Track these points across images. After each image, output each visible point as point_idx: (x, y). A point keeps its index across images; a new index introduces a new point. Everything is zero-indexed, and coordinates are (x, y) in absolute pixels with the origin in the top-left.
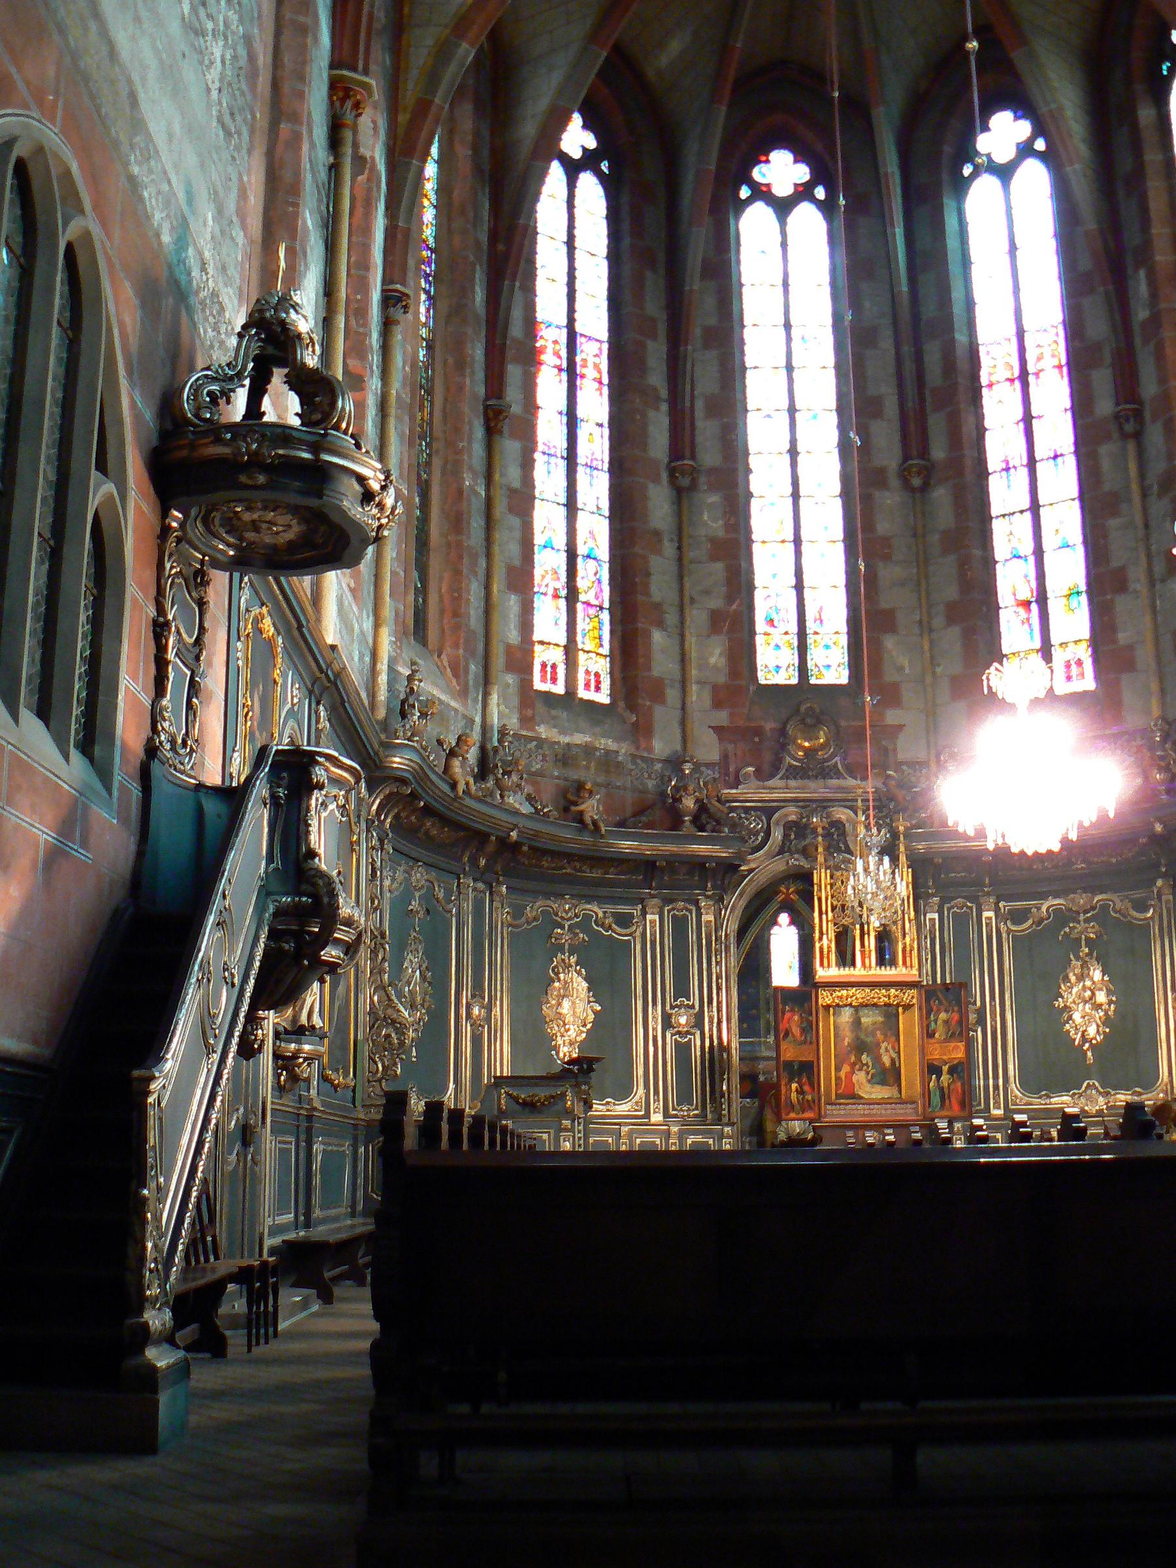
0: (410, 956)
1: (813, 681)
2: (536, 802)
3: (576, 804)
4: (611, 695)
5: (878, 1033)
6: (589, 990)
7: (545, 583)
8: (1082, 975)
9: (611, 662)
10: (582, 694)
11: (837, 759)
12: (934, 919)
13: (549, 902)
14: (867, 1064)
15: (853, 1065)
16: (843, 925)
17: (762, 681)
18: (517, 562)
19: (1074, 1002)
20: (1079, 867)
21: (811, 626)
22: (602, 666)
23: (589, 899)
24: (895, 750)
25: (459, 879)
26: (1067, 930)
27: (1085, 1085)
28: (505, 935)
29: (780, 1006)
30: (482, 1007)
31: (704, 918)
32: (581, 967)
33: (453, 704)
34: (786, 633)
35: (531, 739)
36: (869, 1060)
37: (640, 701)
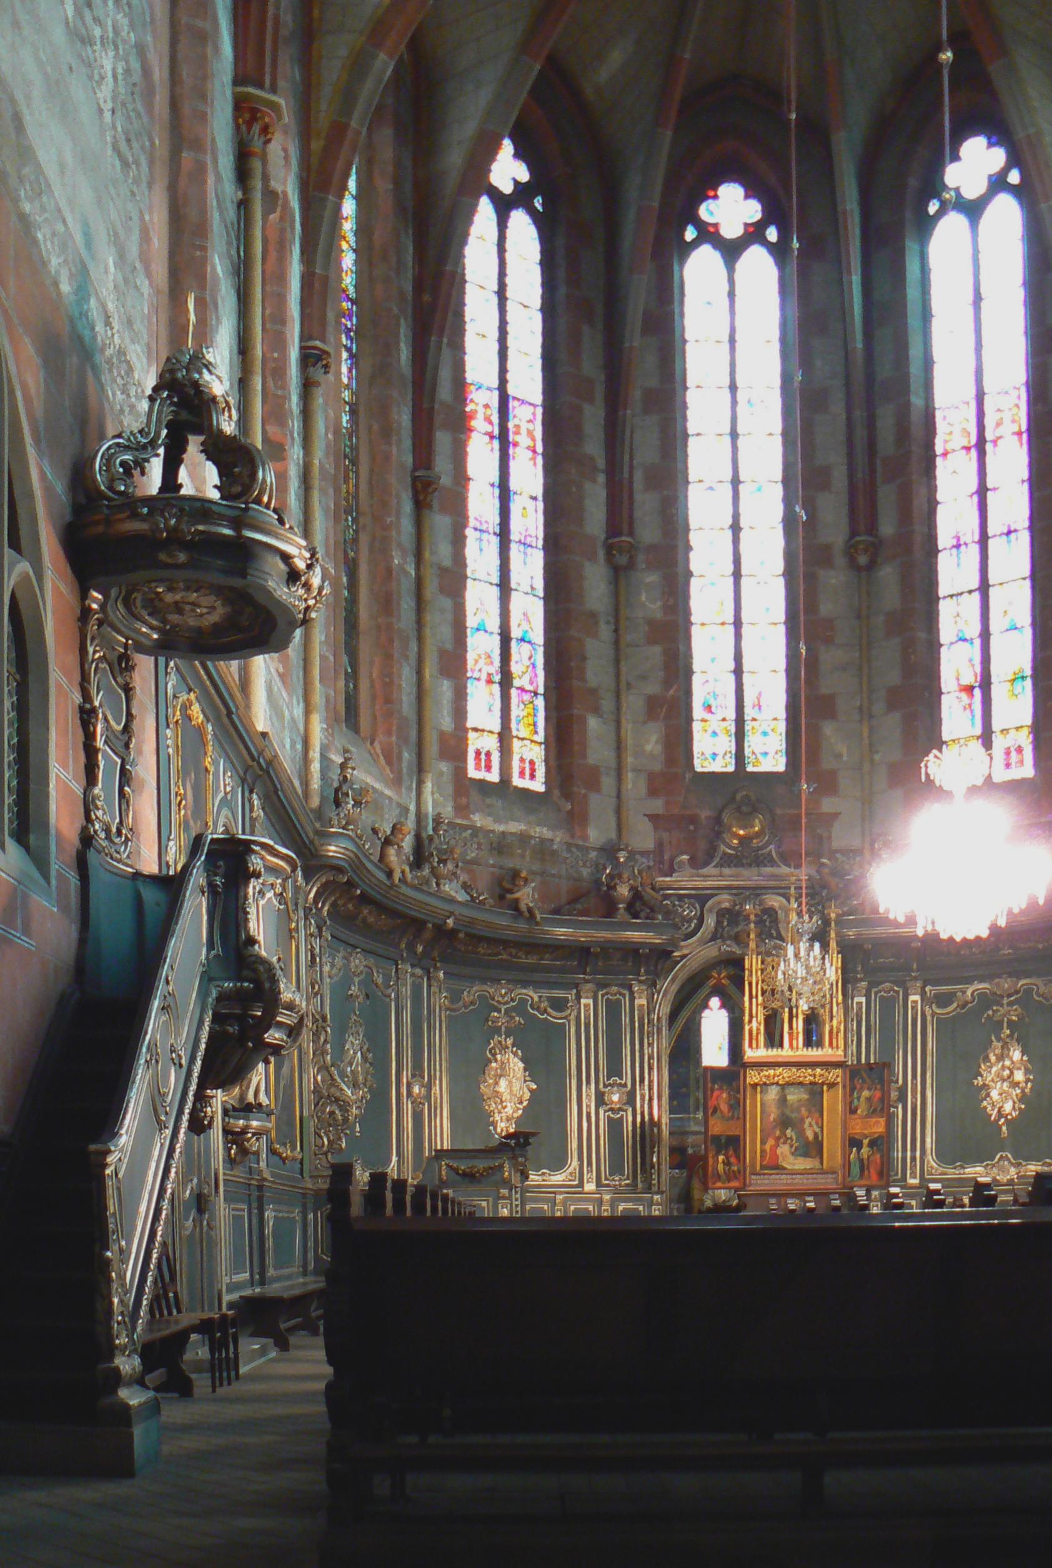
0: (351, 1038)
1: (750, 768)
2: (472, 889)
3: (511, 892)
4: (546, 783)
5: (803, 1109)
7: (477, 668)
9: (546, 750)
10: (517, 782)
11: (772, 847)
12: (861, 1003)
13: (485, 987)
14: (791, 1138)
15: (778, 1139)
16: (773, 1009)
17: (698, 769)
18: (449, 646)
19: (993, 1080)
21: (749, 713)
22: (537, 754)
24: (830, 838)
25: (397, 965)
27: (998, 1156)
29: (710, 1085)
33: (387, 792)
34: (724, 720)
35: (465, 828)
36: (793, 1134)
37: (576, 789)
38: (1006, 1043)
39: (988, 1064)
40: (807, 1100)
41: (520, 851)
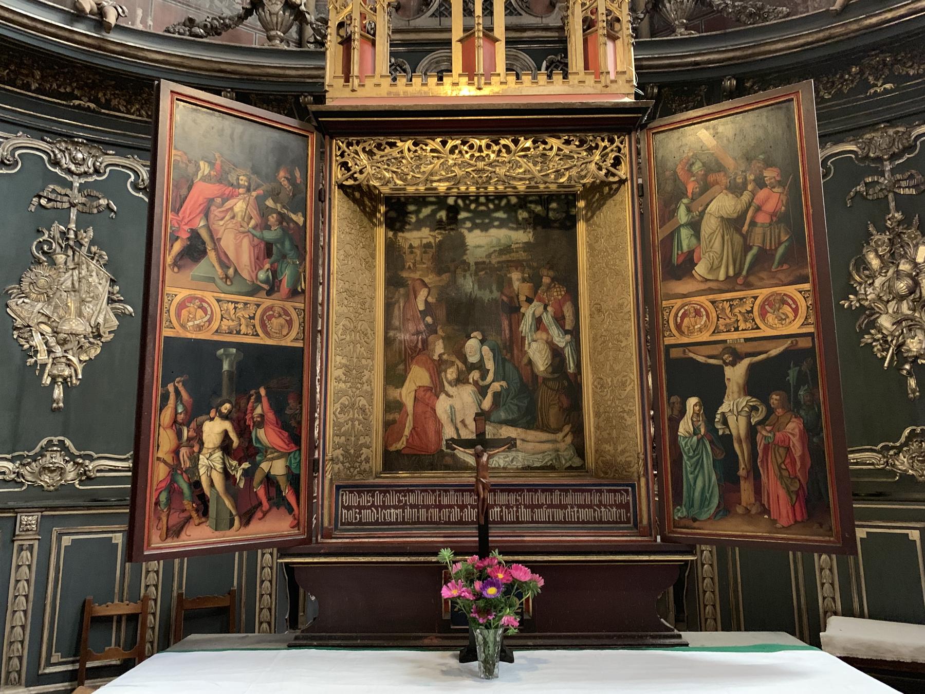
6: (113, 282)
14: (480, 366)
15: (438, 367)
27: (907, 432)
38: (899, 235)
39: (867, 272)
40: (527, 247)
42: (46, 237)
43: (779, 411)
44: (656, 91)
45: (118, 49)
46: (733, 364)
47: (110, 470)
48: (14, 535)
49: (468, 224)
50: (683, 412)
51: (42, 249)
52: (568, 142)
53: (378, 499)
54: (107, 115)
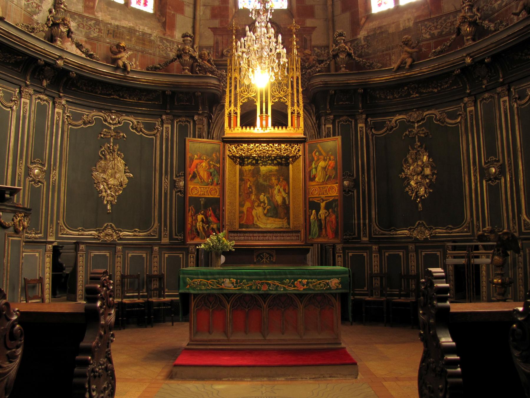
6: (126, 165)
8: (416, 158)
14: (264, 202)
15: (253, 203)
16: (248, 98)
19: (411, 174)
20: (414, 96)
23: (128, 114)
24: (311, 40)
26: (407, 133)
27: (417, 223)
28: (66, 129)
30: (41, 170)
31: (197, 126)
32: (121, 152)
35: (91, 19)
37: (168, 10)
38: (418, 151)
39: (408, 164)
40: (277, 170)
41: (128, 37)
42: (103, 149)
43: (331, 213)
44: (333, 92)
45: (131, 79)
46: (322, 202)
47: (127, 236)
48: (116, 252)
49: (261, 164)
50: (312, 213)
51: (102, 153)
52: (286, 145)
53: (239, 235)
54: (122, 100)
